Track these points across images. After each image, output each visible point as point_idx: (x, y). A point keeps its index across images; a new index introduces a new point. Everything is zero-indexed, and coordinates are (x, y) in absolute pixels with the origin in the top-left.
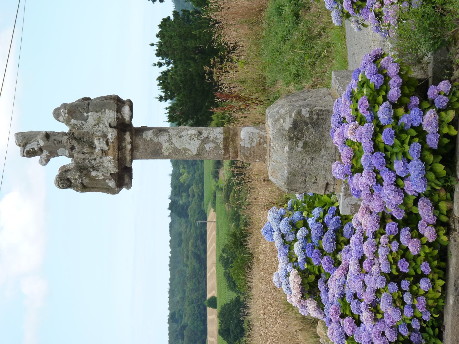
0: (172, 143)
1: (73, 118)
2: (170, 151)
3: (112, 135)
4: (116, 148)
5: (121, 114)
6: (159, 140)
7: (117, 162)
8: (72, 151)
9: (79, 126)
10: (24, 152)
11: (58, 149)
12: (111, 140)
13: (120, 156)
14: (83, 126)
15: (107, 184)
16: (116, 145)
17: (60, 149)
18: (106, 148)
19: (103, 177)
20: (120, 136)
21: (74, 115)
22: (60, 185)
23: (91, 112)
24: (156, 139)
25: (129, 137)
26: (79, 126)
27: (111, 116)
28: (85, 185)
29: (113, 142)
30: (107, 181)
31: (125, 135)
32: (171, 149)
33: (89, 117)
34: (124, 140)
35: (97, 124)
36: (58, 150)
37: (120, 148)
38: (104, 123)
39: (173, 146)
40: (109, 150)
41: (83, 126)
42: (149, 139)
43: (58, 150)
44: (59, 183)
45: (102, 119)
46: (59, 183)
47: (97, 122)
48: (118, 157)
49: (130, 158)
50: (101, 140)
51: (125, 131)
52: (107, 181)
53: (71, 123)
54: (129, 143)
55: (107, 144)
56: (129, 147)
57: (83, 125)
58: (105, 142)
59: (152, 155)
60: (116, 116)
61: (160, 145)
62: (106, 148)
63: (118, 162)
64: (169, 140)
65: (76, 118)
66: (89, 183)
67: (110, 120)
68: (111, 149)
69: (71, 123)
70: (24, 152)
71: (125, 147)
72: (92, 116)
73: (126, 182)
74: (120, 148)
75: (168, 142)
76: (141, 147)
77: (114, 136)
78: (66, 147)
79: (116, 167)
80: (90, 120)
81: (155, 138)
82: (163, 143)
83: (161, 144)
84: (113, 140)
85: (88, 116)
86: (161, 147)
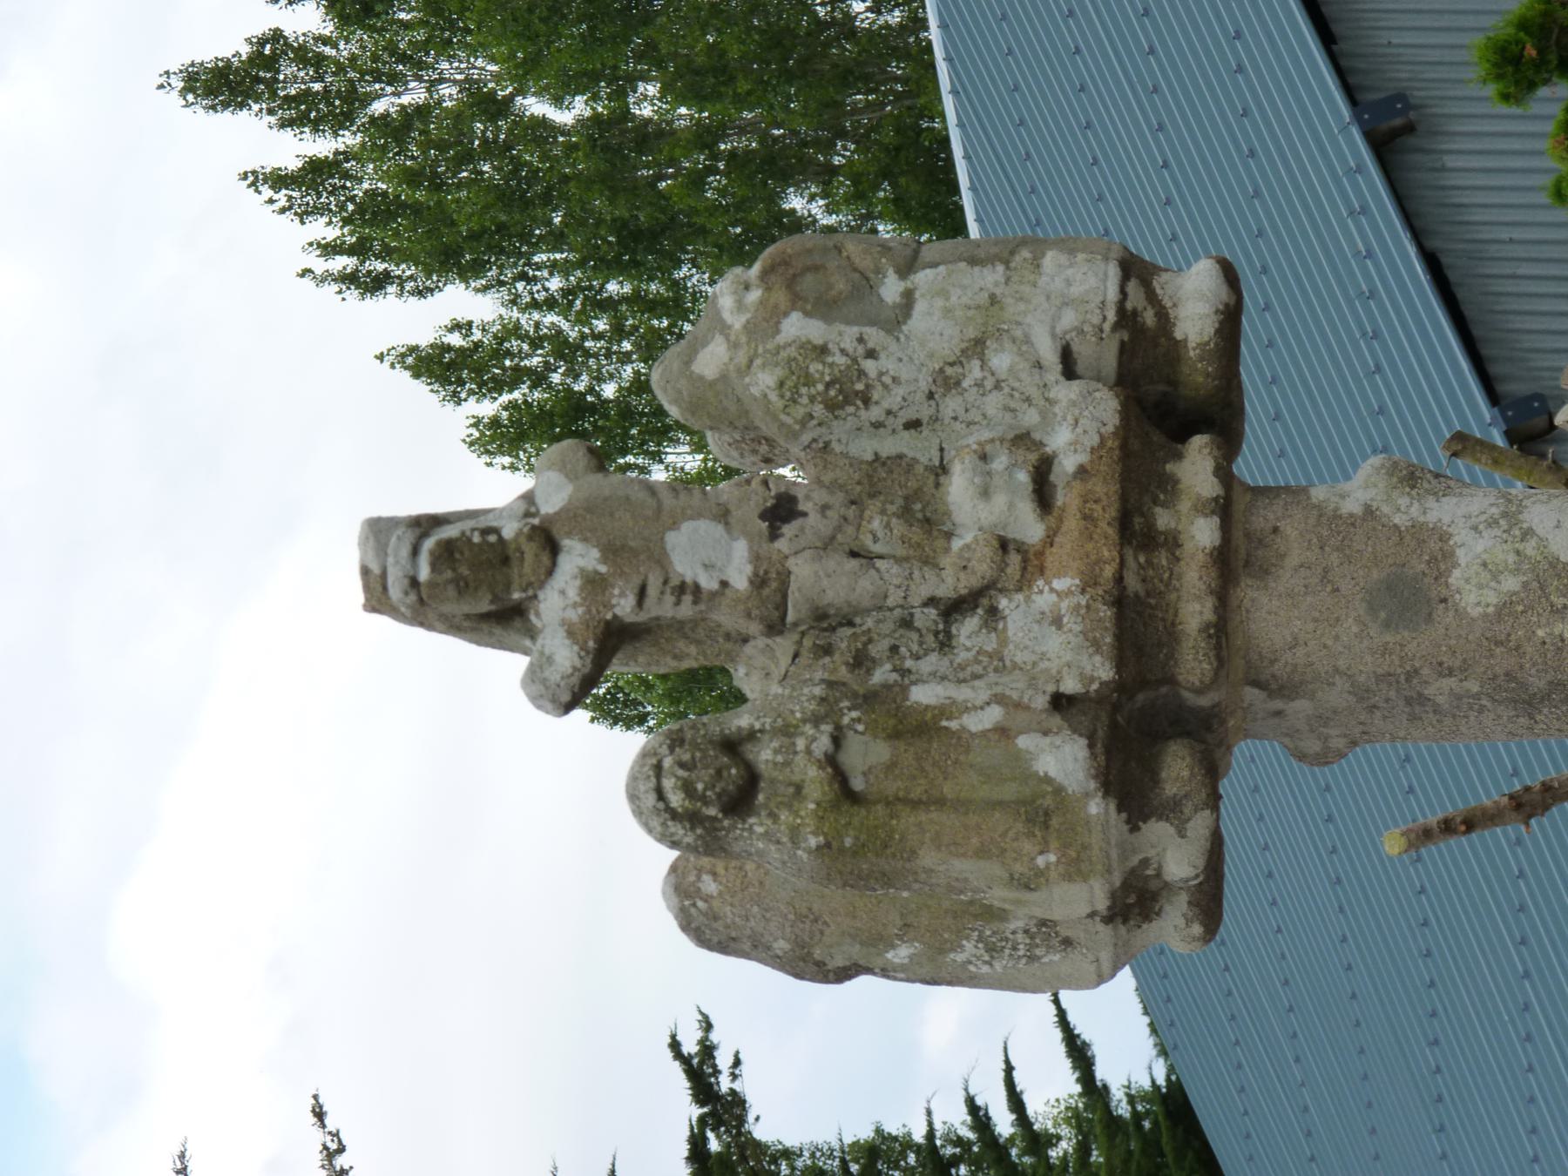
0: (1527, 533)
1: (796, 300)
2: (1511, 583)
3: (1079, 425)
4: (1106, 514)
5: (1152, 297)
6: (1431, 518)
7: (1106, 613)
8: (774, 535)
9: (840, 360)
10: (415, 552)
11: (675, 525)
12: (1068, 463)
13: (1133, 583)
14: (870, 366)
15: (1020, 761)
16: (1106, 489)
17: (687, 527)
18: (1031, 529)
19: (994, 714)
20: (1135, 445)
21: (808, 283)
22: (668, 783)
23: (934, 265)
24: (1405, 510)
25: (1209, 465)
26: (840, 360)
27: (1076, 290)
28: (858, 784)
29: (1082, 472)
30: (1023, 742)
31: (1179, 456)
32: (1516, 571)
33: (920, 307)
34: (1168, 487)
35: (977, 347)
36: (672, 538)
37: (1136, 529)
38: (1027, 340)
39: (1530, 548)
40: (1049, 540)
41: (870, 366)
42: (1357, 509)
43: (672, 538)
44: (658, 768)
45: (1012, 308)
46: (658, 768)
47: (971, 333)
48: (1119, 579)
49: (1209, 615)
50: (1000, 462)
51: (1182, 435)
52: (1023, 742)
53: (781, 339)
54: (1202, 508)
55: (1043, 493)
56: (1203, 533)
57: (871, 354)
58: (1023, 477)
59: (1372, 610)
60: (1112, 294)
61: (1433, 545)
62: (1031, 529)
63: (1120, 618)
64: (1505, 515)
65: (824, 308)
66: (891, 766)
67: (1069, 319)
68: (1072, 523)
69: (781, 339)
70: (415, 552)
71: (1172, 542)
72: (944, 293)
73: (1170, 789)
74: (1136, 529)
75: (1492, 523)
76: (1293, 560)
77: (1092, 427)
78: (736, 513)
79: (1096, 645)
80: (921, 321)
81: (1403, 502)
82: (1461, 534)
83: (1444, 537)
84: (1083, 458)
85: (909, 297)
86: (1443, 558)
